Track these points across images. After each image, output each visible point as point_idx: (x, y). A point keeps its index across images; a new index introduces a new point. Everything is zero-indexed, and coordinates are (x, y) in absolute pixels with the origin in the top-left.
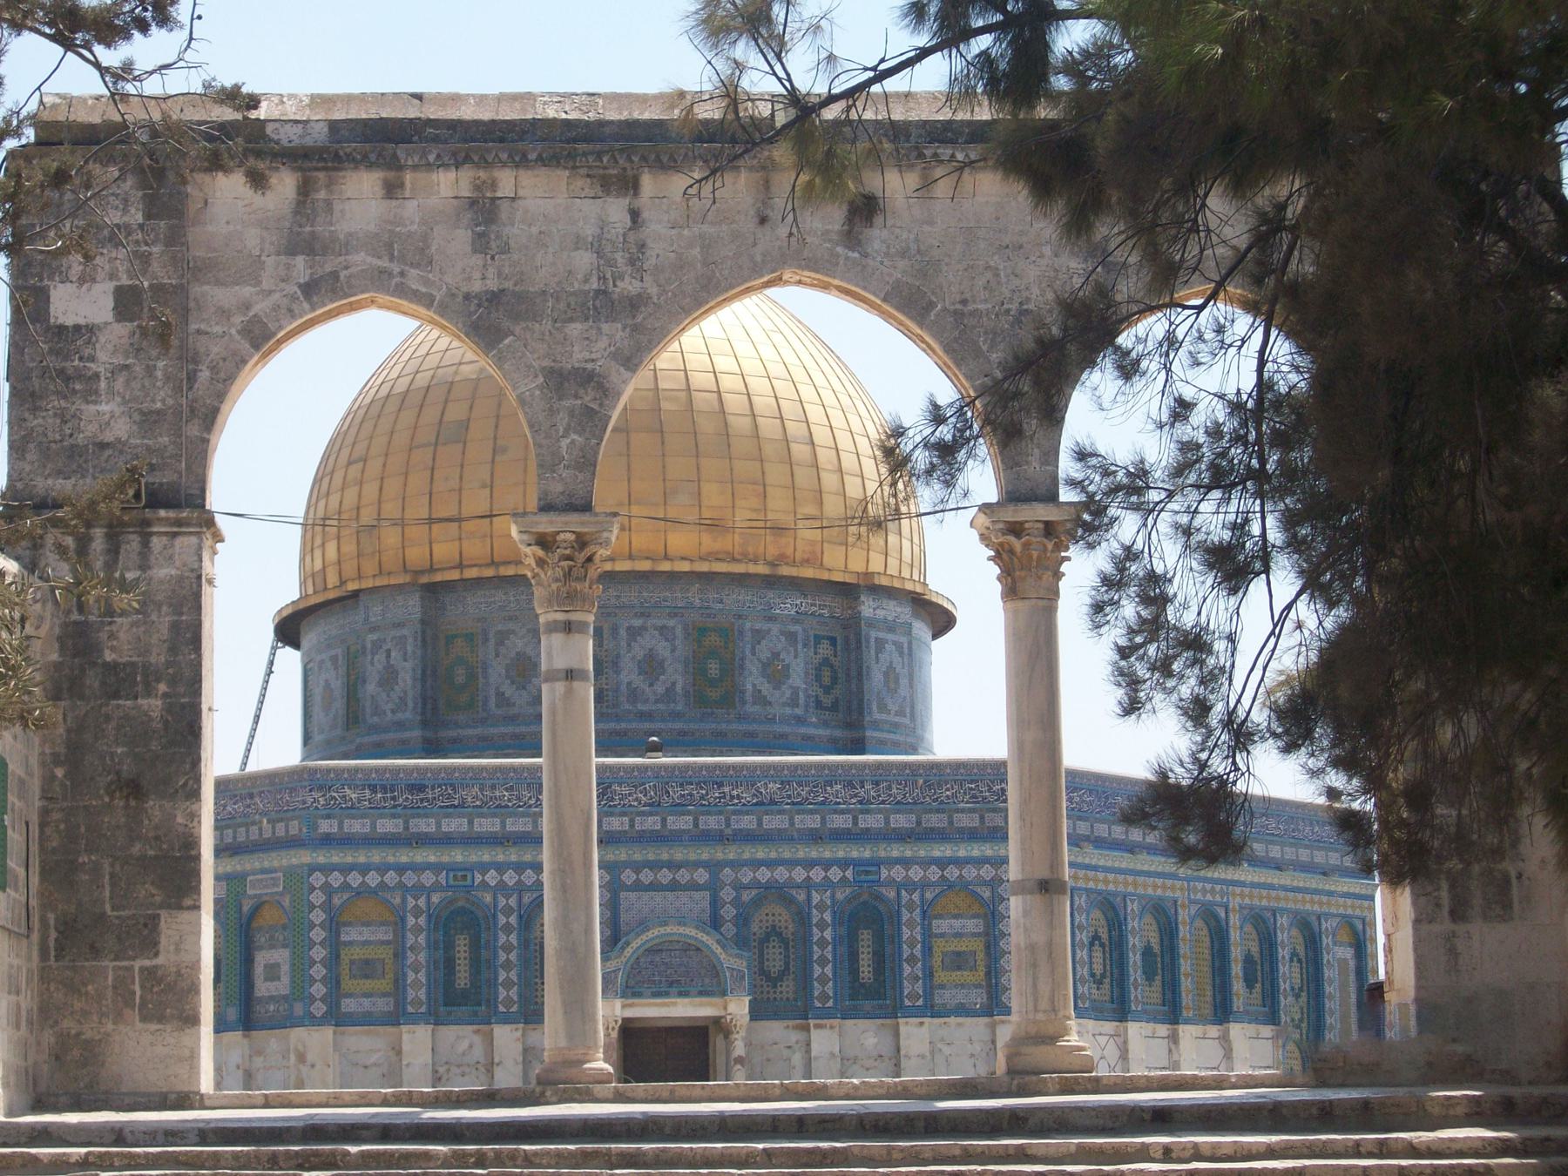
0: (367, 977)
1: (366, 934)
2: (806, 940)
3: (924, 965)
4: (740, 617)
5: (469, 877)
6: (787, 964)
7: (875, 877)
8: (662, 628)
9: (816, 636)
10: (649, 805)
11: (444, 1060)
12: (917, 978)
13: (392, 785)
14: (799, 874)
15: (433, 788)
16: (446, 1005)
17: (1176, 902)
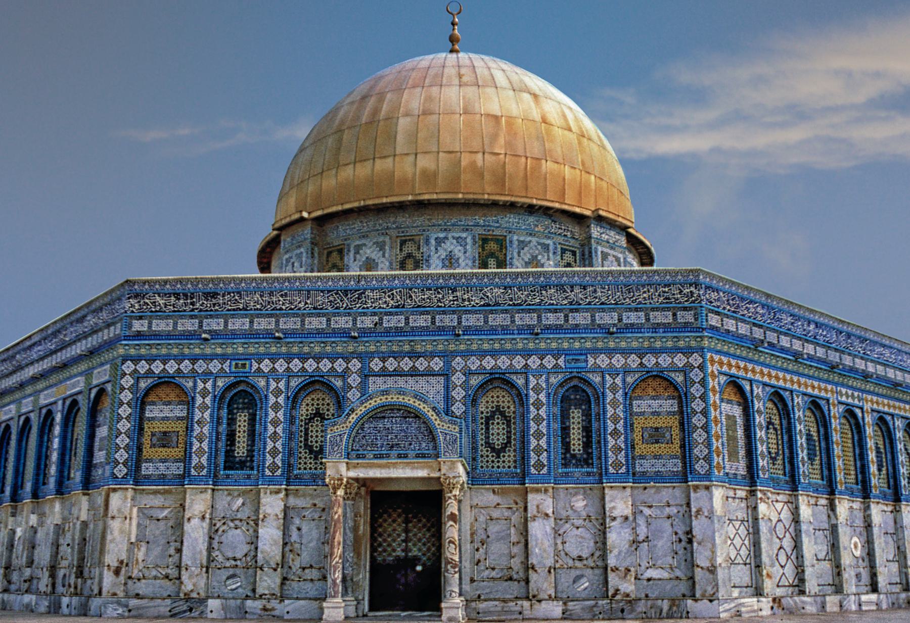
0: (164, 446)
1: (166, 411)
2: (524, 417)
3: (626, 438)
4: (510, 232)
5: (247, 366)
6: (509, 438)
7: (583, 365)
8: (458, 238)
9: (562, 248)
10: (397, 307)
11: (222, 516)
12: (620, 449)
13: (193, 294)
14: (519, 362)
15: (224, 296)
16: (225, 469)
17: (828, 400)
